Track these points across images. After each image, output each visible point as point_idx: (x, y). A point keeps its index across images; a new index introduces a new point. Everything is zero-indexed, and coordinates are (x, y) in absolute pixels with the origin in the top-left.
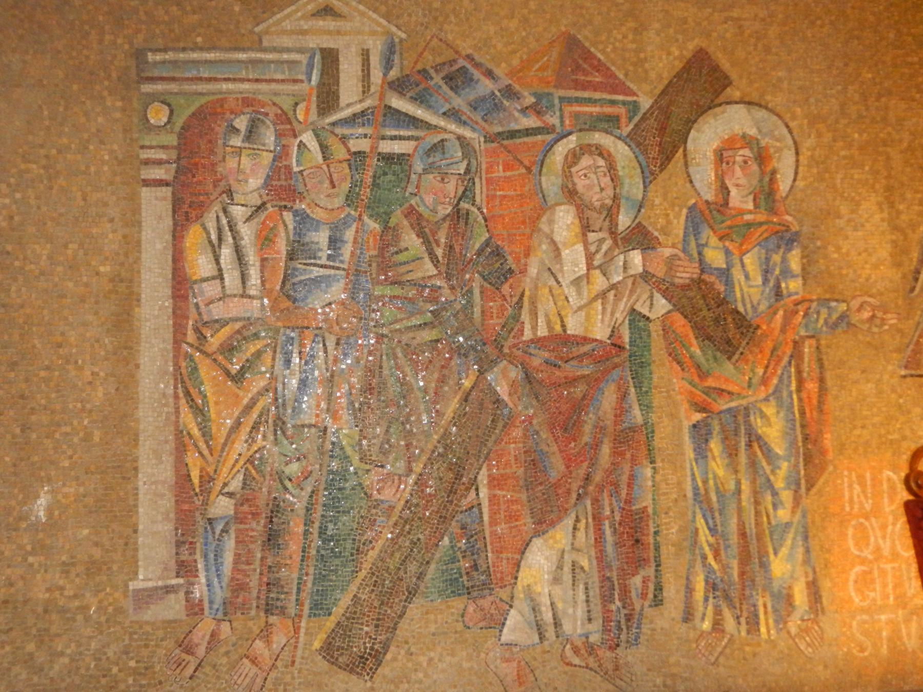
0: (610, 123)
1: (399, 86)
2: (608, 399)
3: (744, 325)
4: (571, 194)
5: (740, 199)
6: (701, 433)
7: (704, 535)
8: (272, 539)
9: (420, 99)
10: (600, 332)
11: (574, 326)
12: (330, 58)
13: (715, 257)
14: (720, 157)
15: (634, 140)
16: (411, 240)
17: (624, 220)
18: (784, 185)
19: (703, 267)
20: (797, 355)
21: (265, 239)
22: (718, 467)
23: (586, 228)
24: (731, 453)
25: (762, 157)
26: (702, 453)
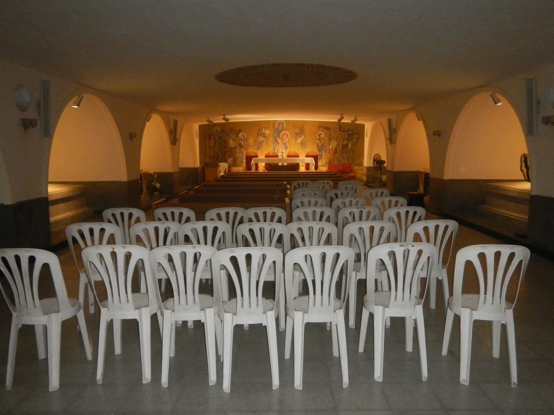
0: (234, 134)
1: (221, 132)
2: (234, 151)
3: (243, 146)
4: (231, 138)
5: (242, 138)
6: (239, 153)
7: (240, 159)
8: (214, 158)
9: (223, 133)
10: (233, 146)
11: (231, 146)
12: (217, 131)
13: (241, 142)
14: (241, 135)
15: (235, 134)
16: (222, 141)
17: (235, 140)
18: (245, 137)
19: (240, 143)
20: (246, 148)
21: (214, 141)
22: (240, 155)
23: (232, 140)
24: (241, 154)
25: (244, 135)
26: (239, 154)
